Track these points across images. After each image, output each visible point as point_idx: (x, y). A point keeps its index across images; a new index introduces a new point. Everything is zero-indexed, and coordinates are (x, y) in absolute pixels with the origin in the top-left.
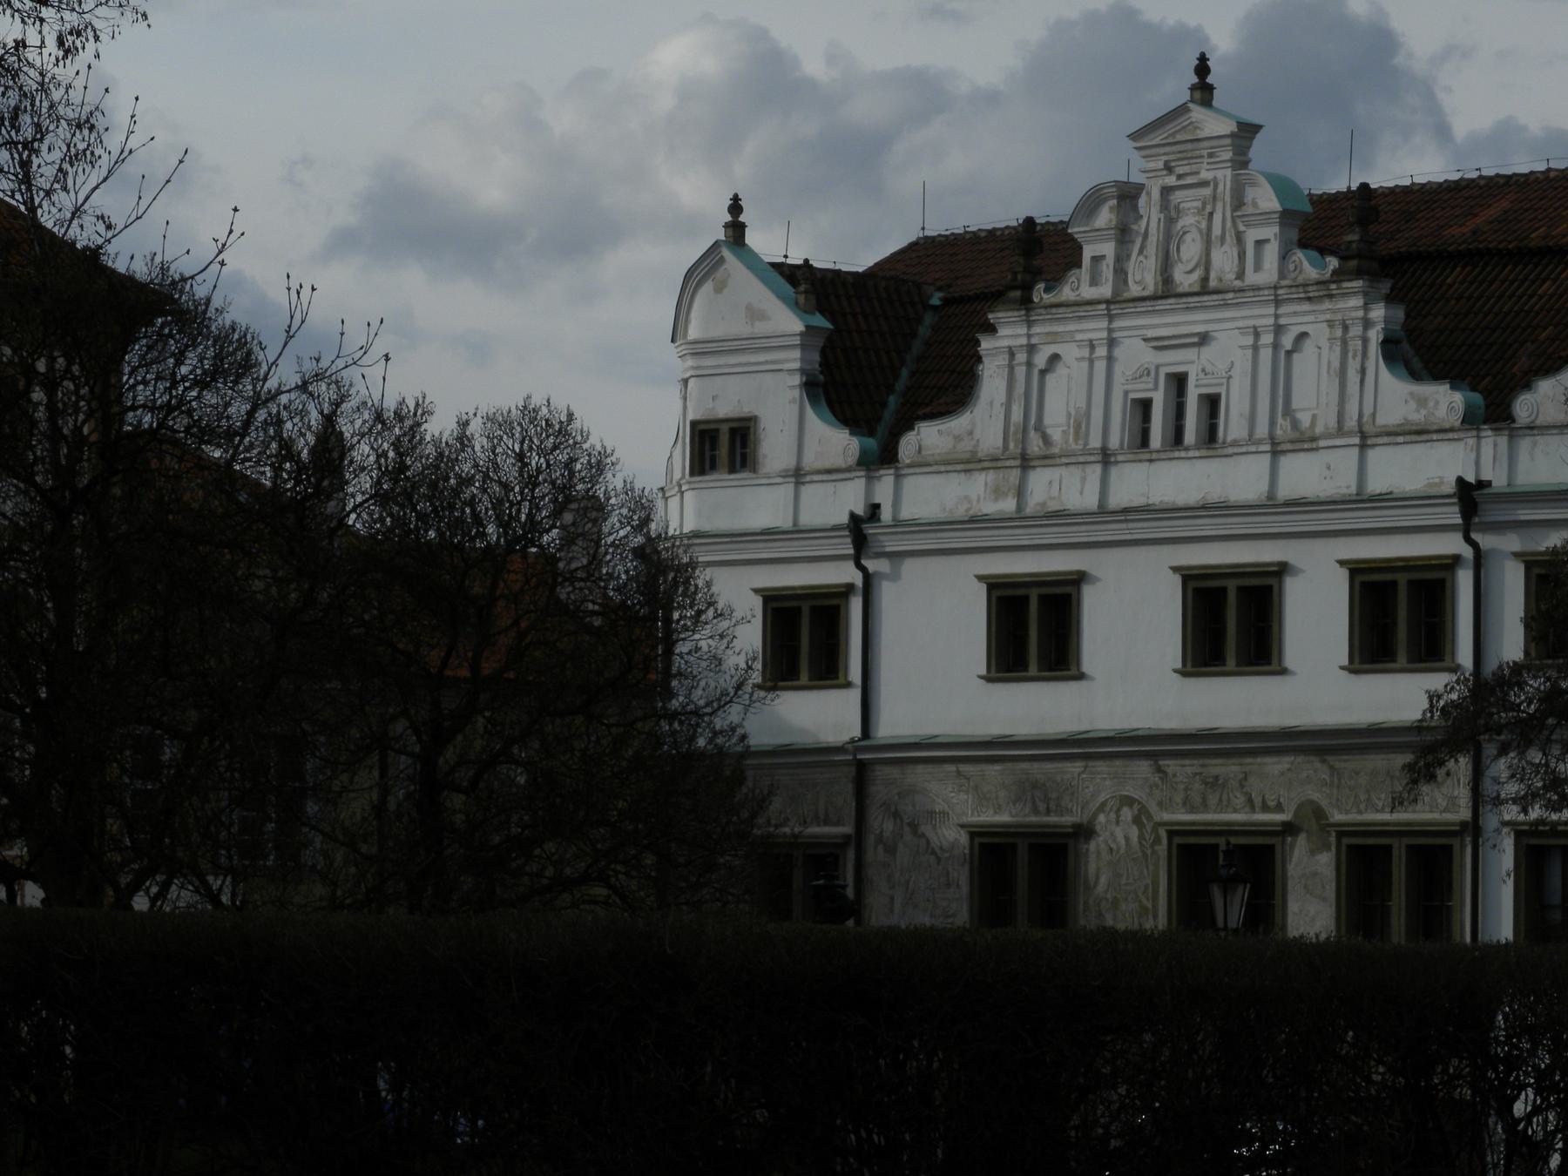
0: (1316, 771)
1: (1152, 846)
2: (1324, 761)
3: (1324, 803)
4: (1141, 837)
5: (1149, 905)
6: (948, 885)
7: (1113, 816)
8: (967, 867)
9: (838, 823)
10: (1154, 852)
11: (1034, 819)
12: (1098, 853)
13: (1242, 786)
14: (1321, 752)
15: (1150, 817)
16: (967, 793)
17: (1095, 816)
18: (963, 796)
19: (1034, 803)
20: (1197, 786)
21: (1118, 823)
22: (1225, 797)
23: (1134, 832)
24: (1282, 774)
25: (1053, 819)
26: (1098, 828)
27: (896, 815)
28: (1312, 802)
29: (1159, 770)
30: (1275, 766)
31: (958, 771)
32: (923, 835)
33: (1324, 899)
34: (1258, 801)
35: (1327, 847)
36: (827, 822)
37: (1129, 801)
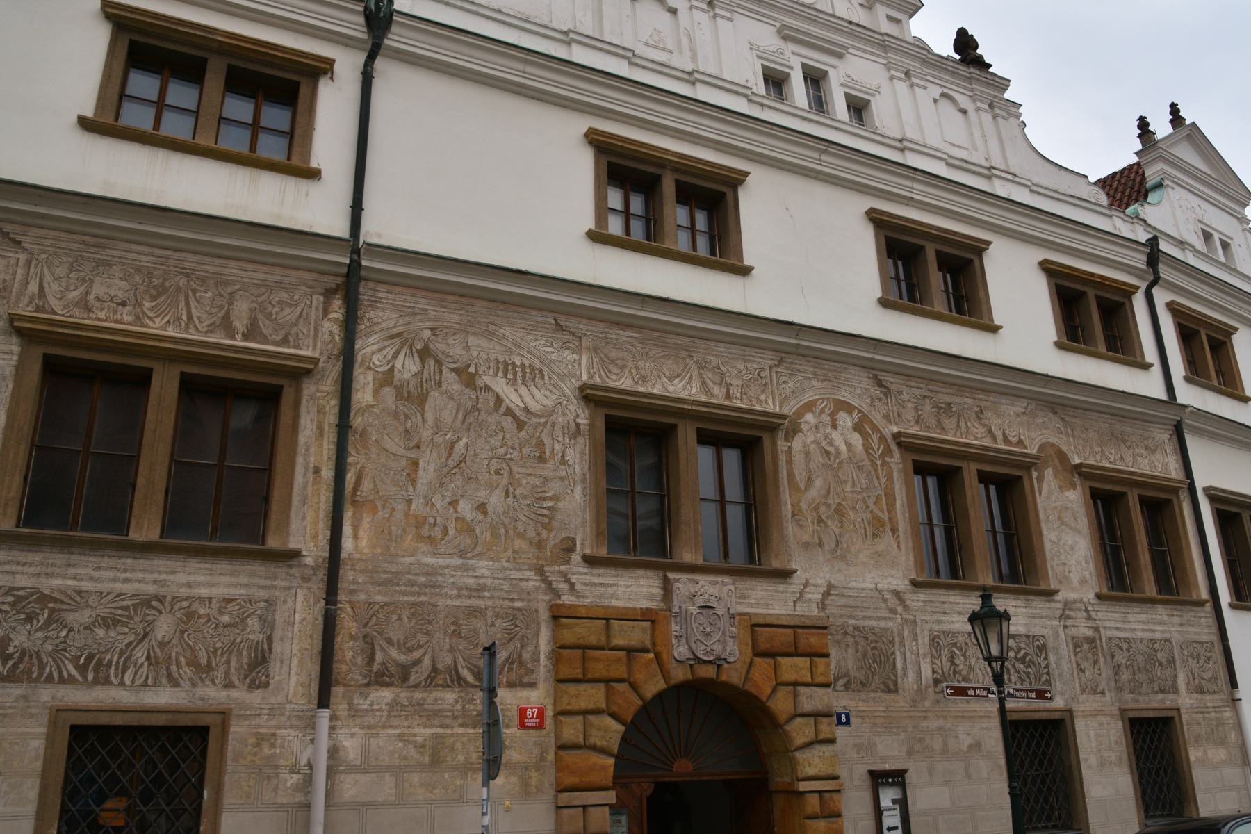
0: (1050, 419)
1: (882, 456)
2: (1055, 413)
3: (1064, 448)
4: (867, 447)
5: (885, 516)
6: (541, 459)
7: (826, 418)
8: (583, 443)
9: (285, 342)
10: (884, 463)
11: (704, 399)
12: (807, 454)
13: (980, 419)
14: (1054, 406)
15: (876, 429)
16: (579, 351)
17: (800, 413)
18: (569, 355)
19: (704, 383)
20: (927, 407)
21: (835, 426)
22: (962, 424)
23: (857, 440)
24: (1018, 415)
25: (736, 403)
26: (804, 427)
27: (424, 354)
28: (1052, 445)
29: (880, 384)
30: (1012, 409)
31: (557, 324)
32: (487, 388)
33: (1079, 532)
34: (999, 434)
35: (1073, 486)
36: (246, 337)
37: (849, 408)
